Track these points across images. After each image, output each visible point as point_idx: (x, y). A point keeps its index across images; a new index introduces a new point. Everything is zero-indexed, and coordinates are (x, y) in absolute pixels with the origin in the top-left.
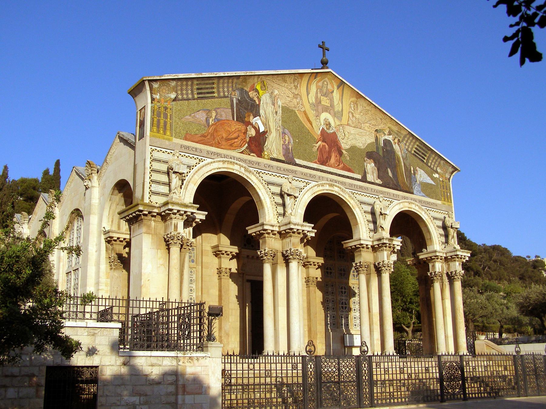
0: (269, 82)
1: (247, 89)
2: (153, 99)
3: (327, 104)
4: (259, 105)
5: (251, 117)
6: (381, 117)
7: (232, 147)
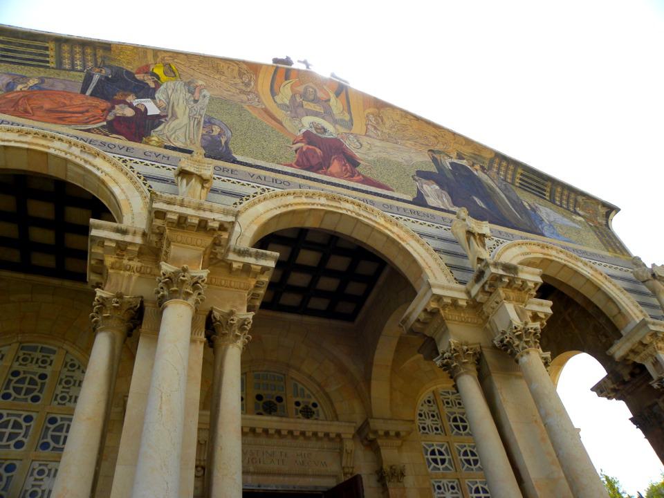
0: (183, 68)
4: (155, 90)
6: (434, 134)
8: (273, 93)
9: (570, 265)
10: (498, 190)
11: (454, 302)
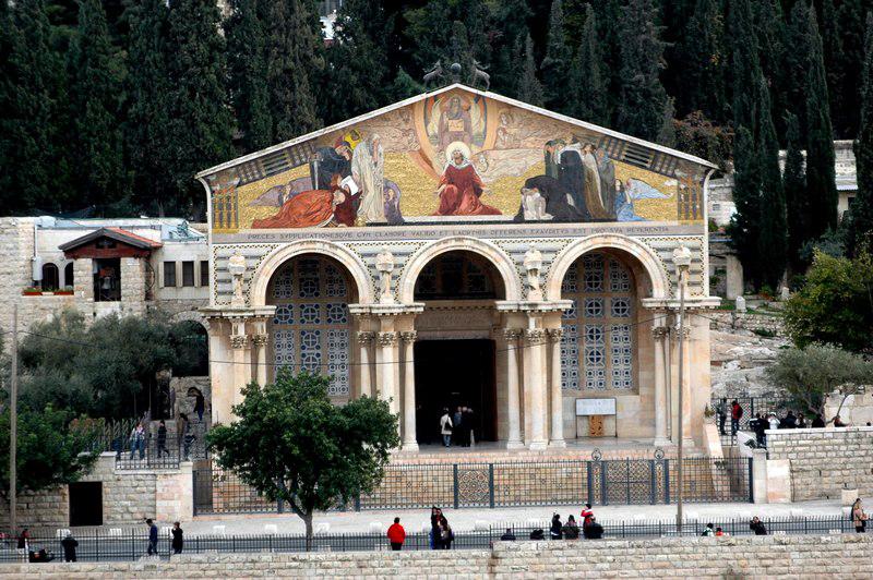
2: (213, 192)
3: (458, 130)
4: (350, 161)
5: (339, 180)
7: (313, 222)
9: (625, 249)
10: (597, 175)
11: (510, 311)
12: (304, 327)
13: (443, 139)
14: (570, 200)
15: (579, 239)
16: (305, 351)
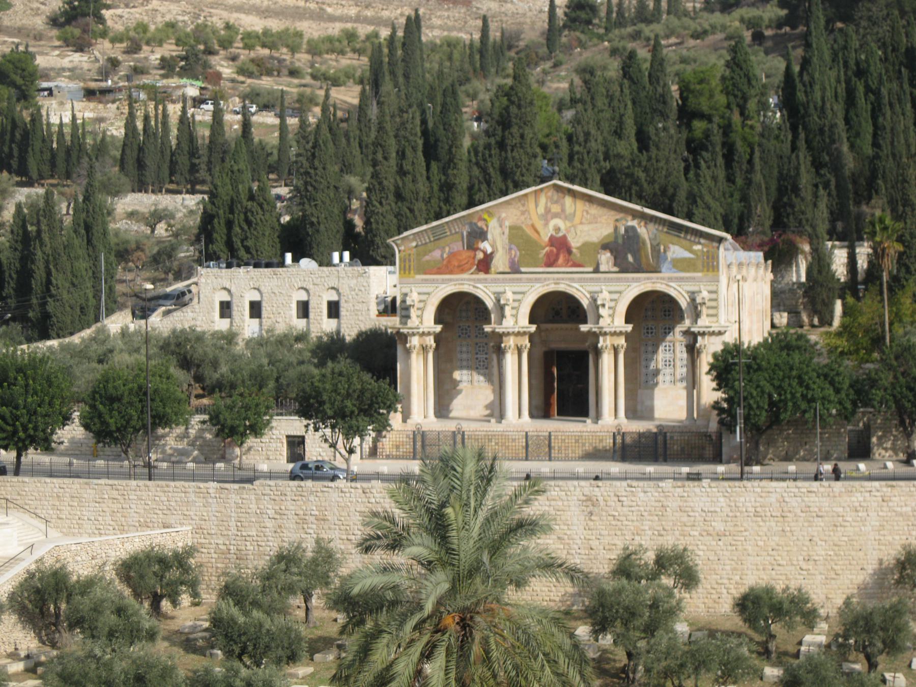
1: (475, 221)
2: (399, 251)
4: (487, 232)
7: (463, 271)
8: (537, 206)
10: (648, 242)
12: (477, 340)
13: (548, 215)
14: (630, 258)
15: (635, 284)
16: (478, 356)
